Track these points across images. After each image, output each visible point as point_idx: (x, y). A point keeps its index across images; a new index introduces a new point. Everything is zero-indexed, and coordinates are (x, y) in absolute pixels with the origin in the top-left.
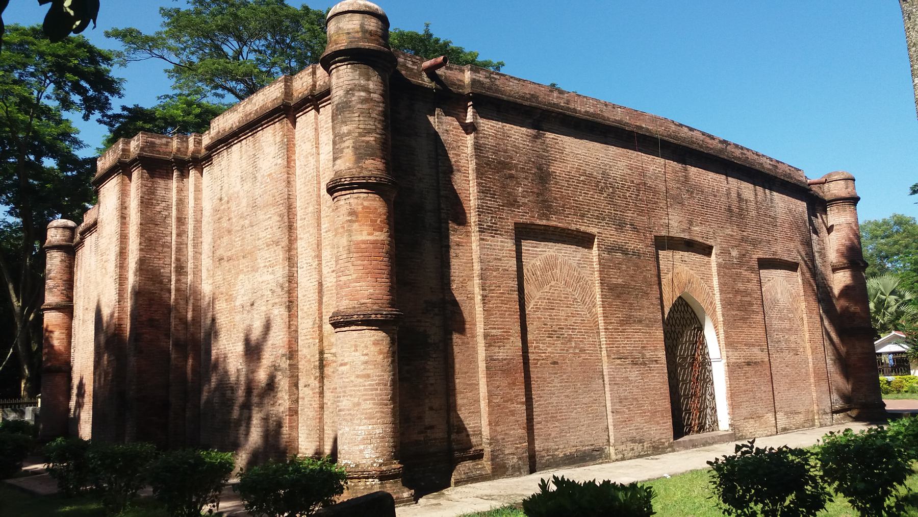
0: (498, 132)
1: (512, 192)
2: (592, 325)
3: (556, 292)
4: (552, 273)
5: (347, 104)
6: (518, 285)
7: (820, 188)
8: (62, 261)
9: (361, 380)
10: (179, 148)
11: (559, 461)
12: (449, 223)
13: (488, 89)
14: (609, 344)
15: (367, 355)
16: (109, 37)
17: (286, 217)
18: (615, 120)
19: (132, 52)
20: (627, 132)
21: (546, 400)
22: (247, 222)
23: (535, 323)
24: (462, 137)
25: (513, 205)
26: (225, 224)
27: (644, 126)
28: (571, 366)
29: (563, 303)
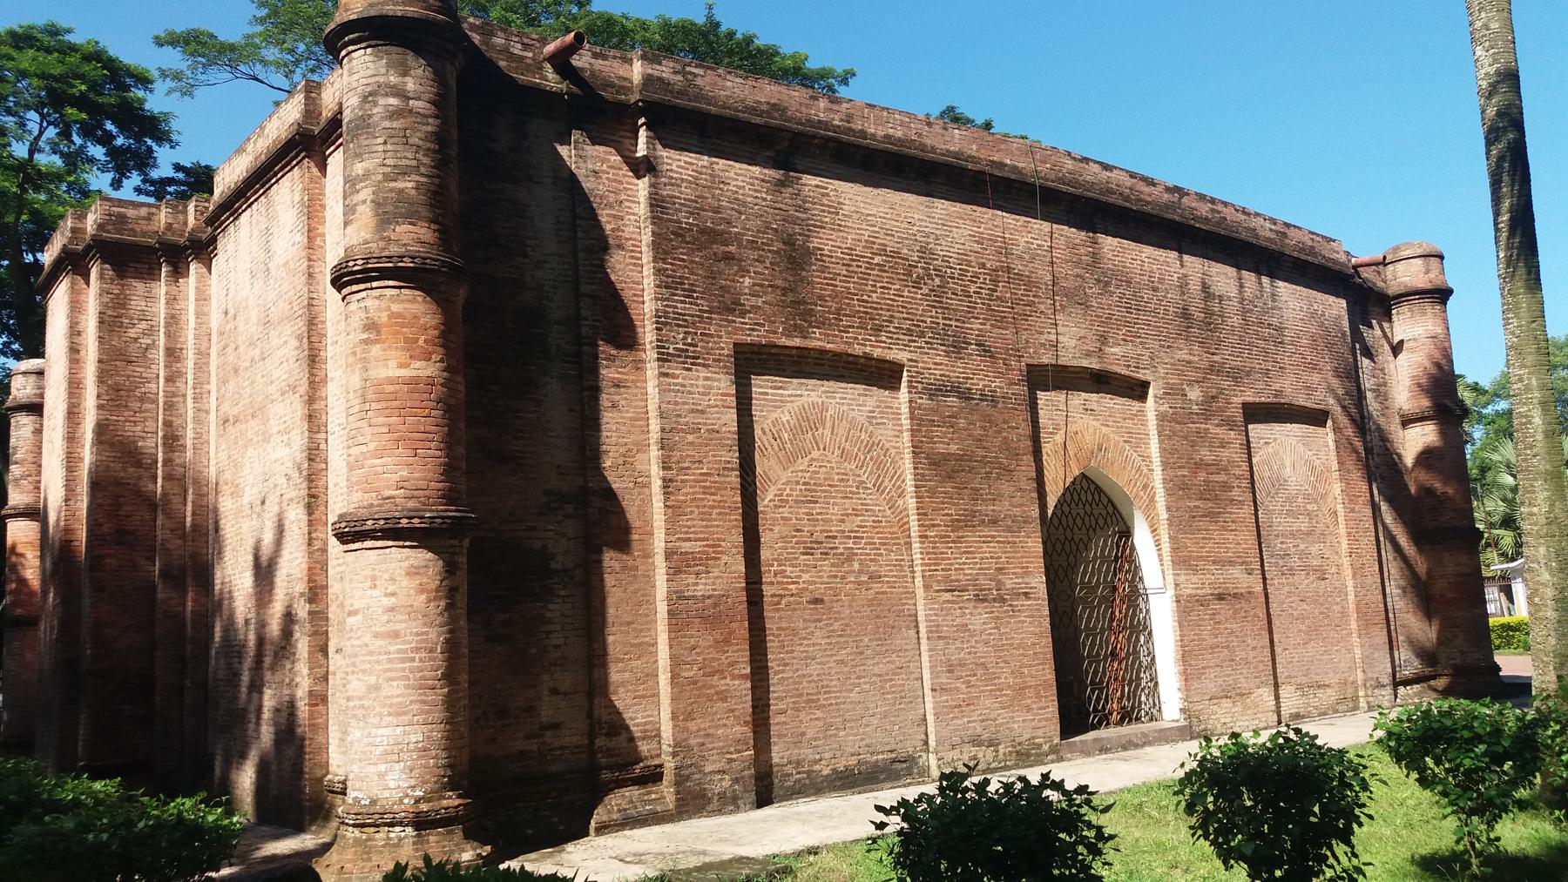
0: (701, 174)
1: (726, 286)
2: (895, 530)
3: (823, 470)
4: (813, 435)
5: (364, 120)
6: (740, 458)
7: (1379, 273)
9: (382, 643)
11: (822, 782)
12: (598, 346)
13: (678, 93)
14: (930, 565)
15: (393, 594)
16: (162, 45)
17: (305, 340)
18: (947, 150)
19: (201, 70)
20: (971, 173)
21: (797, 670)
22: (257, 351)
23: (777, 529)
24: (628, 183)
25: (731, 311)
26: (231, 358)
27: (1008, 162)
28: (850, 606)
29: (836, 491)
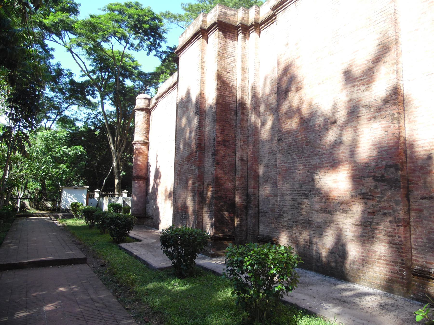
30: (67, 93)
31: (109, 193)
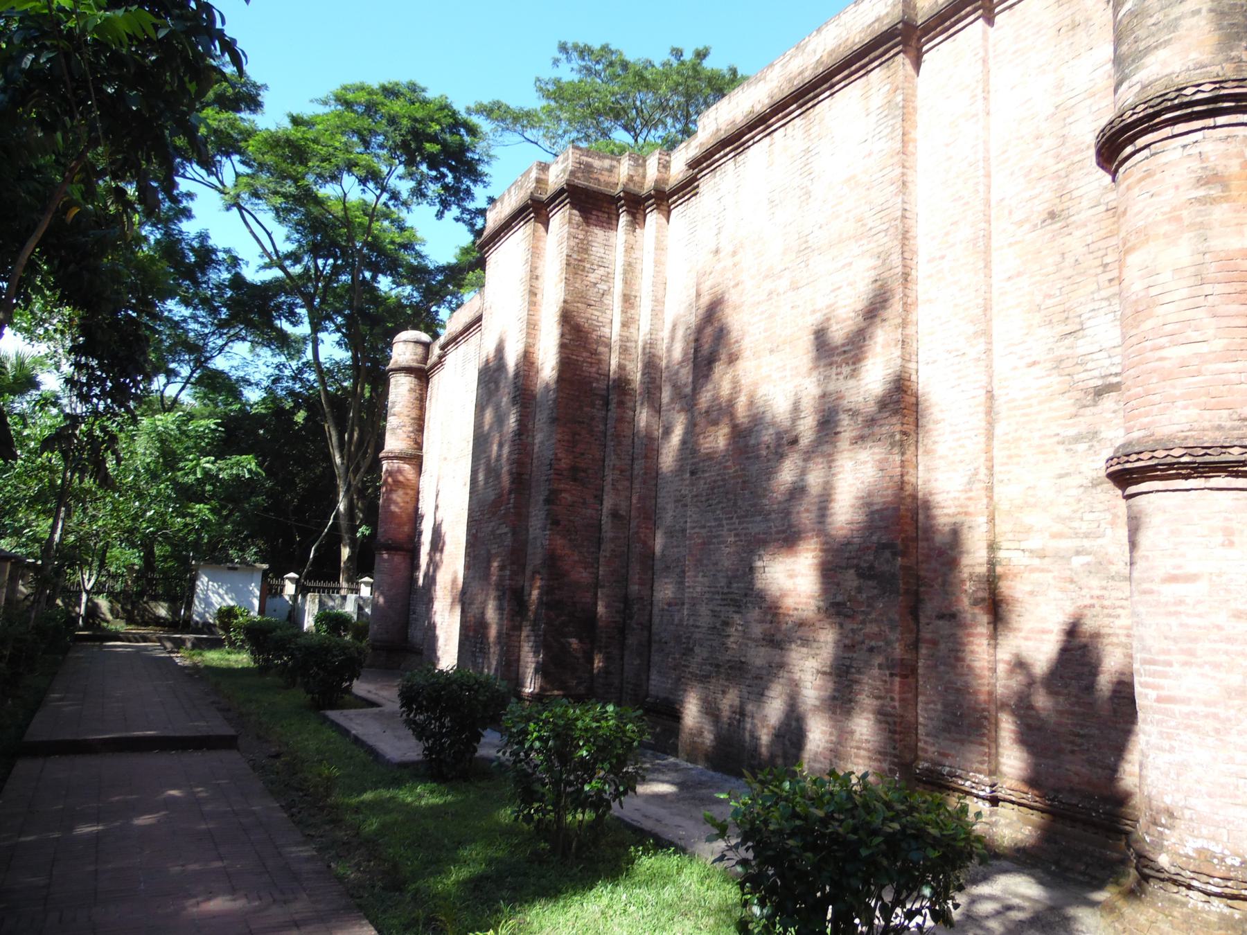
8: (411, 390)
10: (632, 176)
30: (224, 310)
31: (322, 584)
